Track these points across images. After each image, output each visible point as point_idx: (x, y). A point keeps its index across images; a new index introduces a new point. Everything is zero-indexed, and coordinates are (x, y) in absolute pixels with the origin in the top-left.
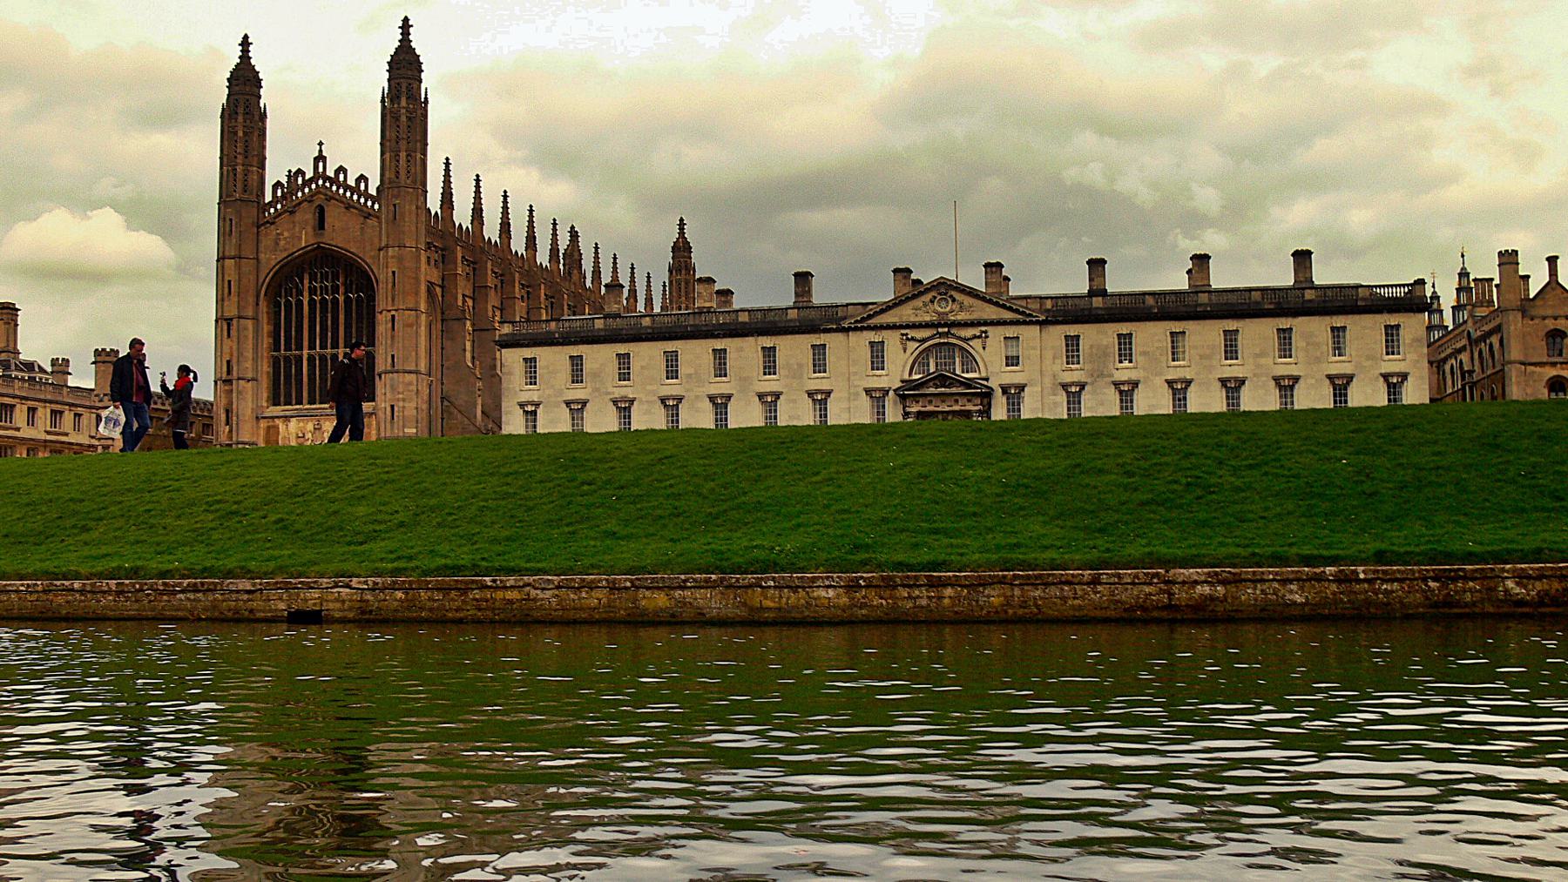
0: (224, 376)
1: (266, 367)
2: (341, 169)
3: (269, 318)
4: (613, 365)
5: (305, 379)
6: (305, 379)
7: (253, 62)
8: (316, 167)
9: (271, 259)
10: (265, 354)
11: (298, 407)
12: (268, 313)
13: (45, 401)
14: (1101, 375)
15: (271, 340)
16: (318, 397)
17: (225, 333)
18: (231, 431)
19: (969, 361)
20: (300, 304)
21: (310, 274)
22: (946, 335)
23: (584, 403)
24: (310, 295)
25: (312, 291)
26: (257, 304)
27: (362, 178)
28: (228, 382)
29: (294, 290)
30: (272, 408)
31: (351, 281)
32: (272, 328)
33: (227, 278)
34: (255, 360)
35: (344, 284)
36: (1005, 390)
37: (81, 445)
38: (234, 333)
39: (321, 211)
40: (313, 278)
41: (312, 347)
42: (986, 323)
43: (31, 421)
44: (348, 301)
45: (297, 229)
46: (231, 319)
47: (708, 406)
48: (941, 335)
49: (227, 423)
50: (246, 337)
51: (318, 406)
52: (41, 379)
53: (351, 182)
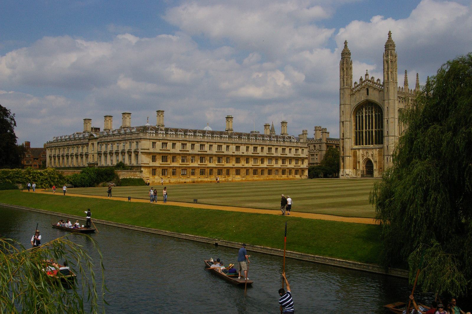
0: (342, 138)
1: (353, 135)
2: (372, 78)
3: (354, 121)
5: (364, 138)
6: (364, 138)
7: (348, 48)
8: (366, 77)
9: (355, 104)
10: (353, 131)
11: (362, 146)
12: (354, 119)
13: (294, 147)
15: (355, 127)
16: (368, 143)
17: (342, 126)
18: (344, 153)
20: (362, 116)
21: (365, 108)
25: (366, 113)
26: (351, 117)
27: (378, 80)
28: (343, 139)
29: (361, 113)
30: (355, 146)
31: (376, 109)
32: (355, 123)
33: (342, 110)
34: (351, 132)
35: (375, 111)
37: (304, 158)
38: (344, 125)
39: (368, 90)
40: (366, 109)
43: (290, 152)
44: (376, 115)
46: (343, 122)
49: (343, 150)
50: (348, 126)
51: (368, 145)
52: (293, 141)
53: (375, 81)
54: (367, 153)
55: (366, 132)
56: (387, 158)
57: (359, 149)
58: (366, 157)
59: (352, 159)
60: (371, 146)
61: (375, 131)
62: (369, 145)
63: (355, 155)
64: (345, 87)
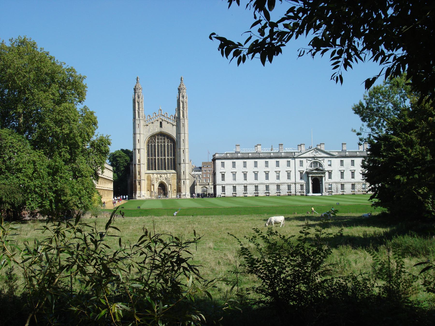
4: (242, 164)
14: (348, 169)
19: (321, 165)
20: (155, 145)
22: (316, 159)
23: (236, 172)
24: (157, 143)
25: (158, 142)
28: (140, 165)
31: (168, 141)
36: (328, 171)
39: (161, 123)
40: (158, 139)
41: (158, 156)
42: (325, 157)
45: (155, 127)
47: (264, 173)
48: (315, 159)
51: (160, 171)
54: (161, 177)
55: (158, 159)
56: (184, 181)
57: (153, 174)
58: (160, 181)
59: (146, 181)
60: (164, 171)
61: (168, 159)
62: (162, 171)
63: (150, 180)
64: (141, 118)
